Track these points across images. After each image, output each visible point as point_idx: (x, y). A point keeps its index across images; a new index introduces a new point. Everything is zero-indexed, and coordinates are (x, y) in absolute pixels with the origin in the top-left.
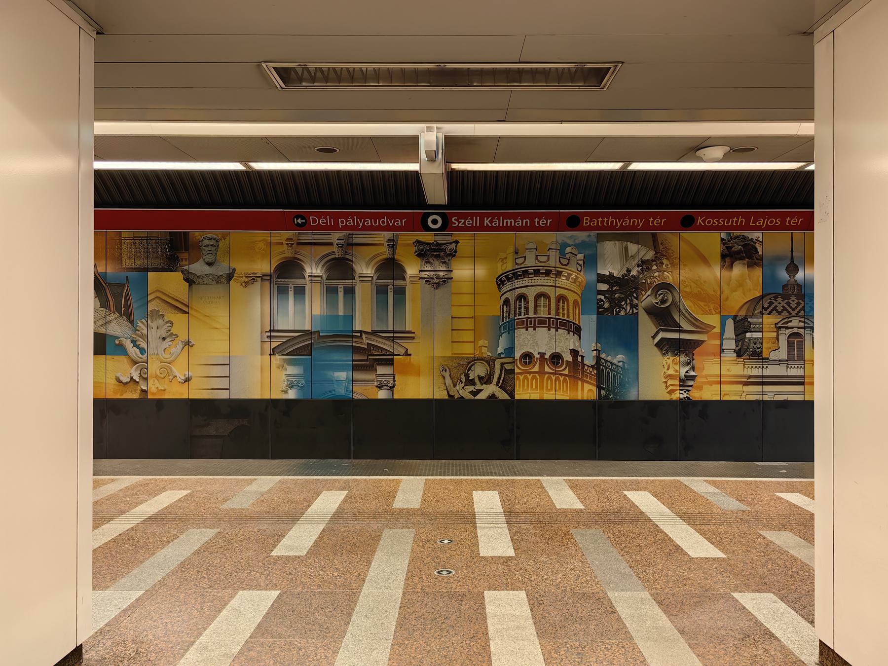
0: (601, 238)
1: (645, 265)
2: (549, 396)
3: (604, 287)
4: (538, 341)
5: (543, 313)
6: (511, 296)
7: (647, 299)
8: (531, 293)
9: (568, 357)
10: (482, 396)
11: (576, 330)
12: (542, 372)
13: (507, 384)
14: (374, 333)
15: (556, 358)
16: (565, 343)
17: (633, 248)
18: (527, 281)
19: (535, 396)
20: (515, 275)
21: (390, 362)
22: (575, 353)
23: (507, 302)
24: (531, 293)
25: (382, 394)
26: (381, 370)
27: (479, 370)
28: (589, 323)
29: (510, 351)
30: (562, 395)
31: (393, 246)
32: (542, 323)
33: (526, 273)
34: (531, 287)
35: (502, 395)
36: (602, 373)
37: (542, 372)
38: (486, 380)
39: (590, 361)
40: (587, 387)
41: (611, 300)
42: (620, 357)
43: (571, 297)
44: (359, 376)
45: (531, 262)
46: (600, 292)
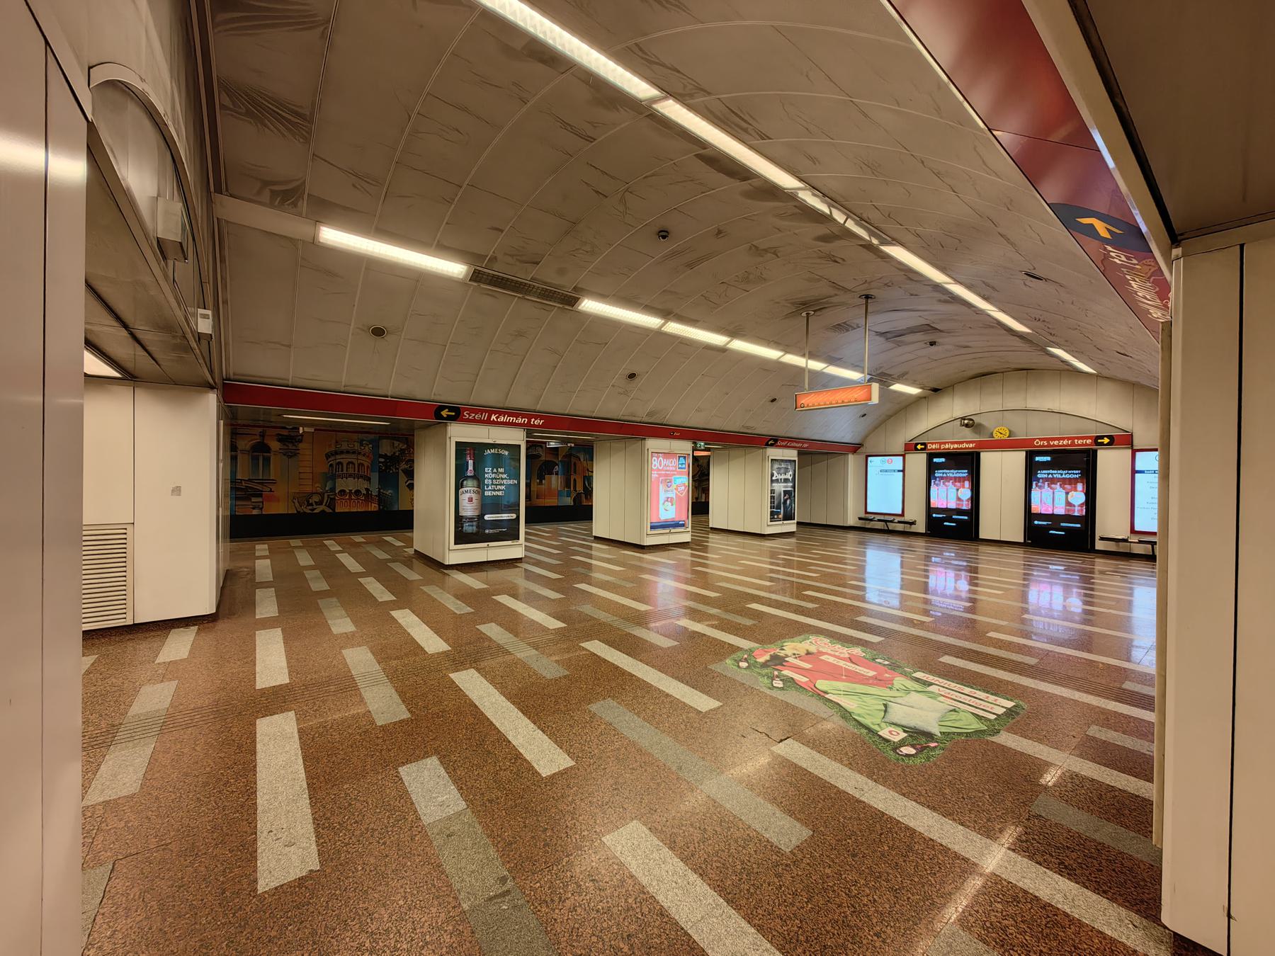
1: (402, 451)
4: (349, 484)
5: (351, 471)
7: (403, 466)
8: (345, 462)
11: (369, 479)
13: (332, 504)
14: (249, 480)
15: (358, 492)
16: (362, 485)
17: (396, 443)
20: (336, 453)
21: (261, 496)
22: (367, 490)
24: (345, 462)
25: (255, 512)
26: (254, 500)
27: (316, 498)
28: (375, 477)
29: (333, 490)
31: (263, 435)
32: (350, 476)
33: (342, 453)
34: (344, 459)
36: (381, 499)
37: (350, 499)
38: (320, 503)
44: (239, 503)
45: (345, 447)
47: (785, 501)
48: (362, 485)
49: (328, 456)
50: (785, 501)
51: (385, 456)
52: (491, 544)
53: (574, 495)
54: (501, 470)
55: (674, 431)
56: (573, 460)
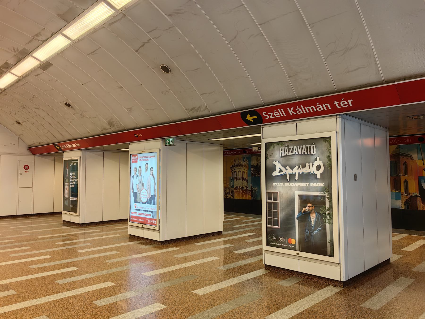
0: (252, 156)
2: (241, 198)
3: (252, 169)
5: (240, 176)
6: (233, 171)
8: (237, 171)
9: (245, 188)
10: (228, 198)
11: (247, 181)
12: (240, 192)
13: (233, 195)
15: (243, 188)
16: (244, 184)
18: (237, 168)
19: (238, 198)
22: (246, 187)
23: (233, 173)
28: (249, 179)
29: (233, 186)
30: (244, 198)
35: (232, 198)
37: (240, 192)
38: (229, 193)
39: (250, 189)
40: (249, 196)
41: (254, 172)
42: (256, 188)
43: (245, 172)
45: (237, 162)
46: (252, 170)
47: (304, 217)
48: (244, 184)
49: (231, 168)
50: (304, 217)
51: (253, 167)
52: (71, 213)
53: (405, 197)
54: (74, 173)
55: (135, 133)
56: (403, 159)
